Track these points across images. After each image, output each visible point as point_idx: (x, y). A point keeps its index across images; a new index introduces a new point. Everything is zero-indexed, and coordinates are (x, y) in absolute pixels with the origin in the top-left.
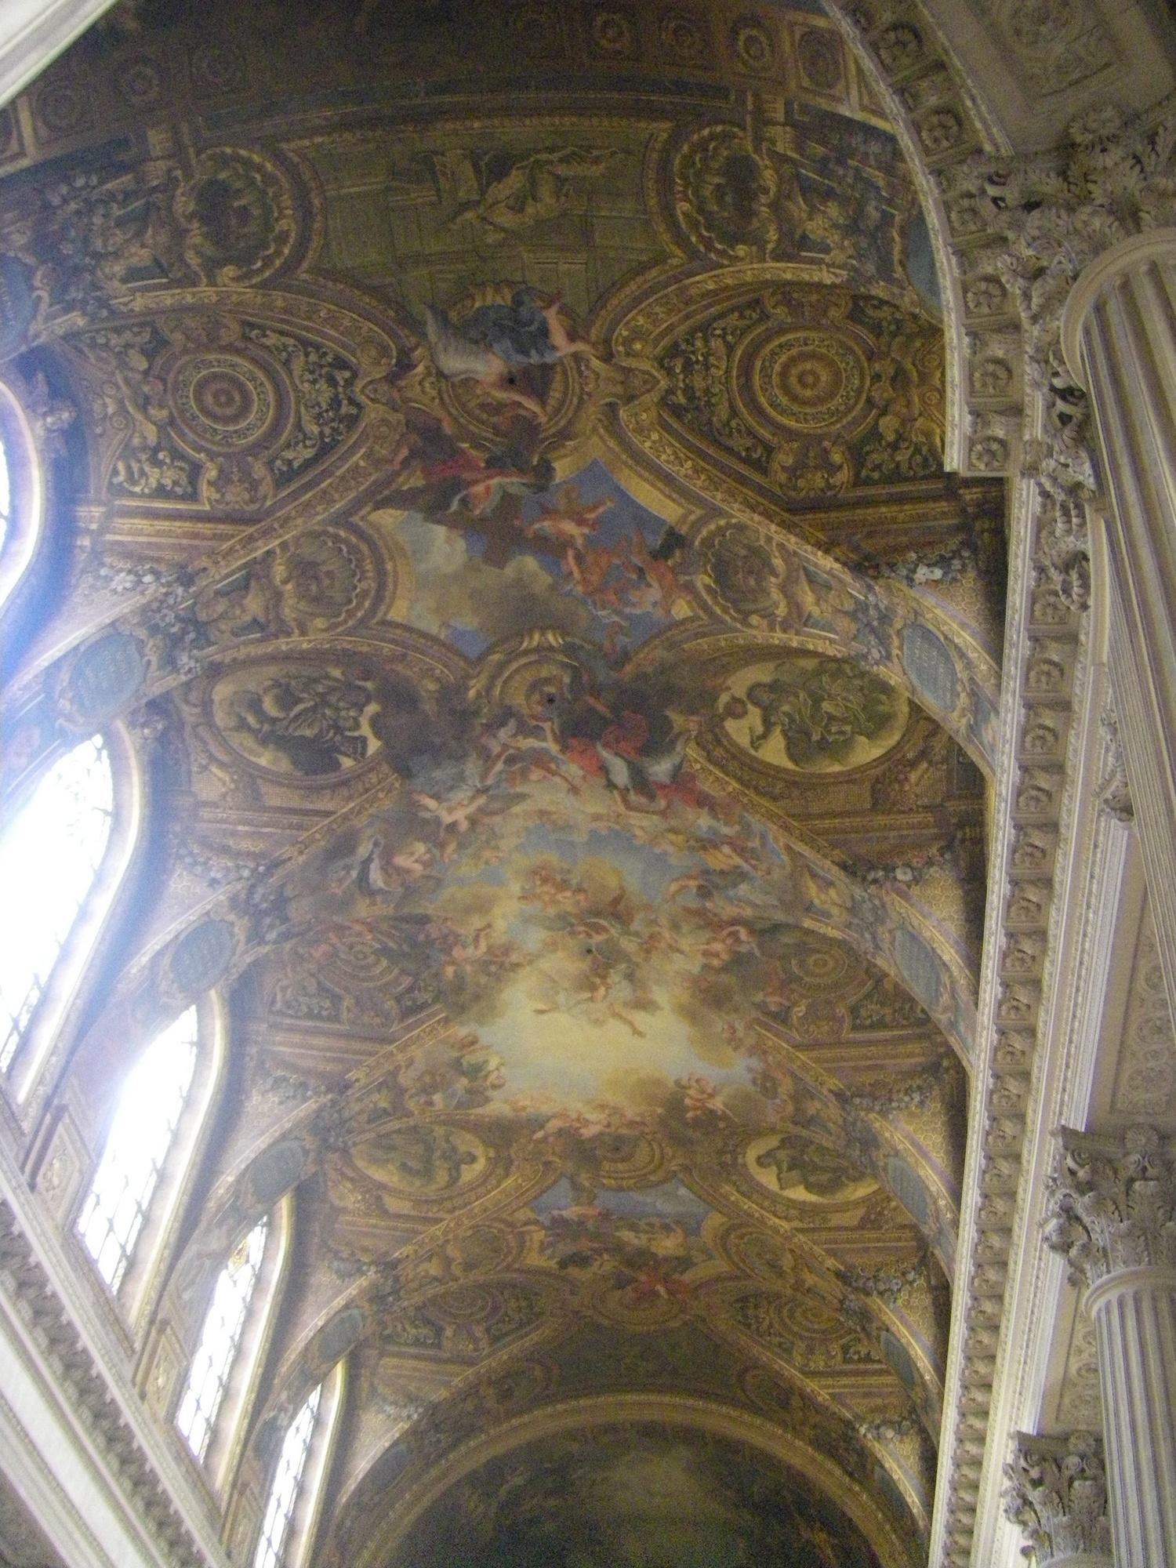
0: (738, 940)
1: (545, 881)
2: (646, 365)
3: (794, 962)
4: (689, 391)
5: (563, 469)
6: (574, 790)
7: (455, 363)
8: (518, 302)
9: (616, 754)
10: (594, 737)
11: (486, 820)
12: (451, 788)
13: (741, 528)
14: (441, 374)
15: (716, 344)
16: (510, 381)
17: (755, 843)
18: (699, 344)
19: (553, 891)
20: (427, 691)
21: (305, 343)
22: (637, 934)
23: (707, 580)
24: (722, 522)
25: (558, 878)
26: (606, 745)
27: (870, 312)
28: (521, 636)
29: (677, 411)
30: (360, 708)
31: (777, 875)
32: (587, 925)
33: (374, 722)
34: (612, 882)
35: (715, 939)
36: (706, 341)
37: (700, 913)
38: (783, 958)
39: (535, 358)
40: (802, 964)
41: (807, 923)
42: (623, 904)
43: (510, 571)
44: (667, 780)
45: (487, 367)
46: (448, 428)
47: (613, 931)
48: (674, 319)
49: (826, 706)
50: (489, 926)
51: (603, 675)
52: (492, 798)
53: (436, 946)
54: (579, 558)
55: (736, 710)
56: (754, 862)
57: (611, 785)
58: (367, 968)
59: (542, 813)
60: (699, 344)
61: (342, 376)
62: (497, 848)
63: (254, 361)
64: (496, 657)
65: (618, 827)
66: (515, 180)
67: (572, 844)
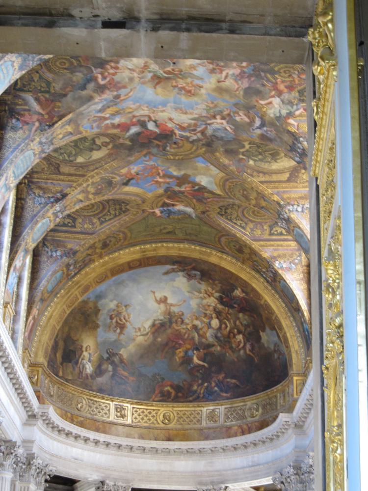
0: (102, 74)
1: (190, 92)
3: (76, 64)
4: (120, 205)
5: (161, 191)
6: (171, 119)
7: (189, 210)
9: (151, 131)
10: (160, 134)
11: (209, 116)
12: (219, 129)
13: (104, 195)
14: (194, 209)
16: (173, 205)
17: (95, 125)
18: (117, 213)
19: (187, 87)
20: (220, 153)
21: (231, 220)
22: (150, 72)
23: (115, 180)
24: (110, 194)
25: (183, 92)
26: (156, 132)
27: (71, 221)
28: (182, 159)
29: (123, 202)
30: (247, 151)
31: (86, 120)
32: (173, 74)
33: (244, 147)
34: (159, 89)
35: (114, 74)
36: (115, 213)
37: (120, 88)
38: (81, 66)
39: (165, 209)
40: (72, 63)
41: (70, 116)
42: (155, 83)
43: (182, 173)
44: (132, 127)
45: (180, 207)
46: (194, 200)
47: (162, 72)
48: (124, 218)
49: (72, 144)
50: (219, 82)
51: (154, 150)
52: (204, 121)
53: (247, 75)
54: (159, 174)
55: (106, 144)
56: (95, 118)
57: (155, 122)
58: (286, 67)
59: (186, 113)
60: (117, 213)
62: (207, 106)
63: (247, 218)
64: (192, 156)
65: (154, 109)
66: (165, 231)
67: (175, 103)
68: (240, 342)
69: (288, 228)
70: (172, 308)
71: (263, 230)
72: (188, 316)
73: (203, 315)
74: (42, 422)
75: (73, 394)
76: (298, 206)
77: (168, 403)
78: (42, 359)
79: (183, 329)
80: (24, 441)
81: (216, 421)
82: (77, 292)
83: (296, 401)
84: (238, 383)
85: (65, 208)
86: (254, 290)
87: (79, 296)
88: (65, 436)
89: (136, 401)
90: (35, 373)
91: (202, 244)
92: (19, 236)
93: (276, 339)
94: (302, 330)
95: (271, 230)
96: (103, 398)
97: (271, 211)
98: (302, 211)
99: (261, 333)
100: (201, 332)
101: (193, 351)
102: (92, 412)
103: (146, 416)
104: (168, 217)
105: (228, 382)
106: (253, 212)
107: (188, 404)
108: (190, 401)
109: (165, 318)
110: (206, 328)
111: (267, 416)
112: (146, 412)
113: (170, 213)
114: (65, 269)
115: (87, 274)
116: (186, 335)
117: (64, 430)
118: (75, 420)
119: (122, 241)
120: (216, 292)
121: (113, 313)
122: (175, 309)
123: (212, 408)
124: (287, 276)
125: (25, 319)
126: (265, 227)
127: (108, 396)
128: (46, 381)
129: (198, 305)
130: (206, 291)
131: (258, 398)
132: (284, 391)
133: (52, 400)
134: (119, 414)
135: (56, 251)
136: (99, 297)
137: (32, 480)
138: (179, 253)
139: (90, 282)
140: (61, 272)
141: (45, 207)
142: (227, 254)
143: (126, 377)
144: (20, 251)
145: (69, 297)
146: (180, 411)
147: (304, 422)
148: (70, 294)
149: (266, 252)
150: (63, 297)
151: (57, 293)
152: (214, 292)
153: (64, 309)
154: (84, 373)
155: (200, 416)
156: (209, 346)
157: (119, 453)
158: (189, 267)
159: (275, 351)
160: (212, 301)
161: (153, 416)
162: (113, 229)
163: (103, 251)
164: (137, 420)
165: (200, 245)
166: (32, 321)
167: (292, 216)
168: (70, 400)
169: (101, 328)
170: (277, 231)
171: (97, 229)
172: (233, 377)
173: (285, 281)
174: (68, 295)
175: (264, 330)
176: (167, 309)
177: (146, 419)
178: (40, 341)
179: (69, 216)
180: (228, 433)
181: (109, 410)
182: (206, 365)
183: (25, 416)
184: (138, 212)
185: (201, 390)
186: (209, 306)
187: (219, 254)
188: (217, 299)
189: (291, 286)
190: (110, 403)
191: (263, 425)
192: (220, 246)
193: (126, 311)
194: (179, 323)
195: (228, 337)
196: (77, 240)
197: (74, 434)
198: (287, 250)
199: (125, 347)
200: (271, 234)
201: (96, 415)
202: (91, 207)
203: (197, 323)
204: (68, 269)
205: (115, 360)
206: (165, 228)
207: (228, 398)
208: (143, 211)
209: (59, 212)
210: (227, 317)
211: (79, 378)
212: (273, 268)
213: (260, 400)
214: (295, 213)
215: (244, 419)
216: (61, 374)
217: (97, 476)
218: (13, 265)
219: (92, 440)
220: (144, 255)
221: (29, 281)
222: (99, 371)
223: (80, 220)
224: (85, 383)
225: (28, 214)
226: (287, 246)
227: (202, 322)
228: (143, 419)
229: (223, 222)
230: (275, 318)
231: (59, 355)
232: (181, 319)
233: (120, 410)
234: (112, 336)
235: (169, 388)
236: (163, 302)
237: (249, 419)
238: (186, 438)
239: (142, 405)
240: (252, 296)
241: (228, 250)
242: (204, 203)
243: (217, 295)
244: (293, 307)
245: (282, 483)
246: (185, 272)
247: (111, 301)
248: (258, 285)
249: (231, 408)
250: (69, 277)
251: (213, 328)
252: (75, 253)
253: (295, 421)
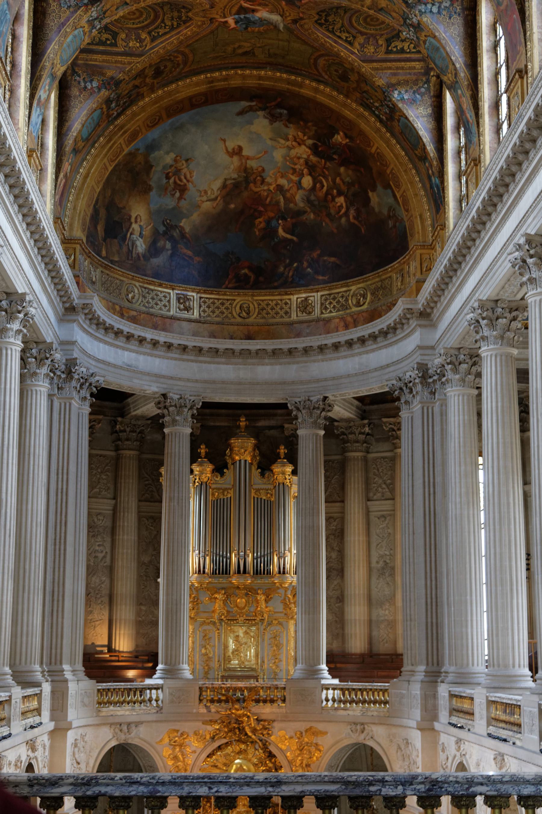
2: (197, 18)
4: (179, 11)
7: (275, 18)
8: (246, 28)
14: (282, 16)
15: (169, 23)
16: (254, 11)
18: (175, 23)
21: (333, 32)
27: (110, 37)
29: (184, 7)
36: (172, 25)
39: (242, 16)
45: (263, 14)
48: (185, 31)
60: (175, 23)
61: (323, 21)
63: (356, 29)
66: (240, 51)
68: (341, 206)
69: (417, 38)
70: (248, 162)
71: (378, 46)
72: (272, 172)
73: (291, 171)
74: (83, 317)
75: (121, 280)
76: (433, 5)
77: (246, 291)
78: (78, 233)
79: (264, 190)
80: (62, 343)
81: (310, 313)
82: (121, 140)
83: (420, 283)
84: (338, 262)
85: (104, 13)
86: (362, 133)
87: (124, 146)
88: (113, 335)
89: (204, 288)
90: (71, 251)
91: (291, 70)
92: (43, 54)
93: (391, 200)
94: (428, 186)
95: (388, 46)
96: (160, 285)
97: (394, 14)
98: (439, 12)
99: (370, 194)
100: (288, 195)
101: (278, 221)
102: (147, 304)
103: (218, 308)
104: (246, 28)
105: (325, 261)
106: (365, 20)
107: (272, 291)
108: (276, 288)
109: (239, 176)
110: (295, 189)
111: (379, 304)
112: (218, 303)
113: (248, 23)
114: (104, 106)
115: (134, 115)
116: (268, 199)
117: (112, 327)
118: (125, 314)
119: (181, 66)
120: (309, 138)
121: (170, 170)
122: (252, 164)
123: (304, 295)
124: (410, 112)
125: (54, 177)
126: (380, 42)
127: (167, 283)
128: (86, 263)
129: (284, 158)
130: (294, 137)
131: (367, 281)
132: (402, 270)
133: (94, 289)
134: (182, 306)
135: (91, 81)
136: (152, 147)
137: (75, 393)
138: (259, 84)
139: (139, 126)
140: (99, 111)
141: (76, 11)
142: (326, 84)
143: (190, 257)
144: (44, 77)
145: (111, 148)
146: (263, 301)
147: (432, 308)
148: (112, 142)
149: (381, 78)
150: (103, 147)
151: (95, 142)
152: (305, 138)
153: (104, 164)
154: (134, 252)
155: (288, 306)
156: (300, 213)
157: (185, 357)
158: (273, 103)
159: (389, 217)
160: (303, 151)
161: (227, 308)
162: (169, 48)
163: (155, 81)
164: (206, 314)
165: (286, 72)
166: (64, 181)
167: (425, 19)
168: (117, 288)
169: (154, 191)
170: (396, 47)
171: (147, 48)
172: (330, 255)
173: (406, 118)
174: (110, 145)
175: (374, 189)
176: (242, 163)
177: (217, 312)
178: (75, 208)
179: (106, 28)
180: (325, 325)
181: (169, 301)
182: (295, 238)
183: (60, 308)
184: (204, 23)
185: (289, 273)
186: (299, 158)
187: (314, 84)
188: (309, 148)
189: (415, 125)
190: (171, 291)
191: (373, 315)
192: (316, 73)
193: (187, 167)
194: (259, 183)
195: (325, 199)
196: (119, 65)
197: (125, 333)
198: (410, 74)
199: (187, 217)
200: (388, 52)
201: (152, 307)
202: (137, 14)
203: (283, 182)
204: (109, 108)
205: (175, 234)
206: (240, 47)
207: (325, 282)
208: (212, 20)
209: (95, 19)
210: (324, 172)
211: (128, 259)
212: (390, 101)
213: (369, 283)
214: (428, 15)
215: (347, 308)
216: (104, 253)
217: (157, 387)
218: (37, 97)
219: (148, 340)
220: (211, 87)
221: (56, 124)
222: (153, 250)
223: (123, 36)
224: (136, 266)
225: (52, 22)
226: (410, 68)
227: (290, 181)
228: (213, 312)
229: (322, 36)
230: (391, 172)
231: (100, 228)
232: (261, 176)
233: (182, 300)
234: (169, 202)
235: (246, 271)
236: (236, 154)
237: (354, 309)
238: (271, 335)
239: (212, 294)
240: (358, 142)
241: (326, 77)
242: (296, 6)
243: (310, 142)
244: (416, 155)
245: (401, 389)
246: (268, 111)
247: (168, 153)
248: (369, 124)
249: (330, 295)
250: (110, 119)
251: (304, 189)
252: (118, 83)
253: (420, 306)
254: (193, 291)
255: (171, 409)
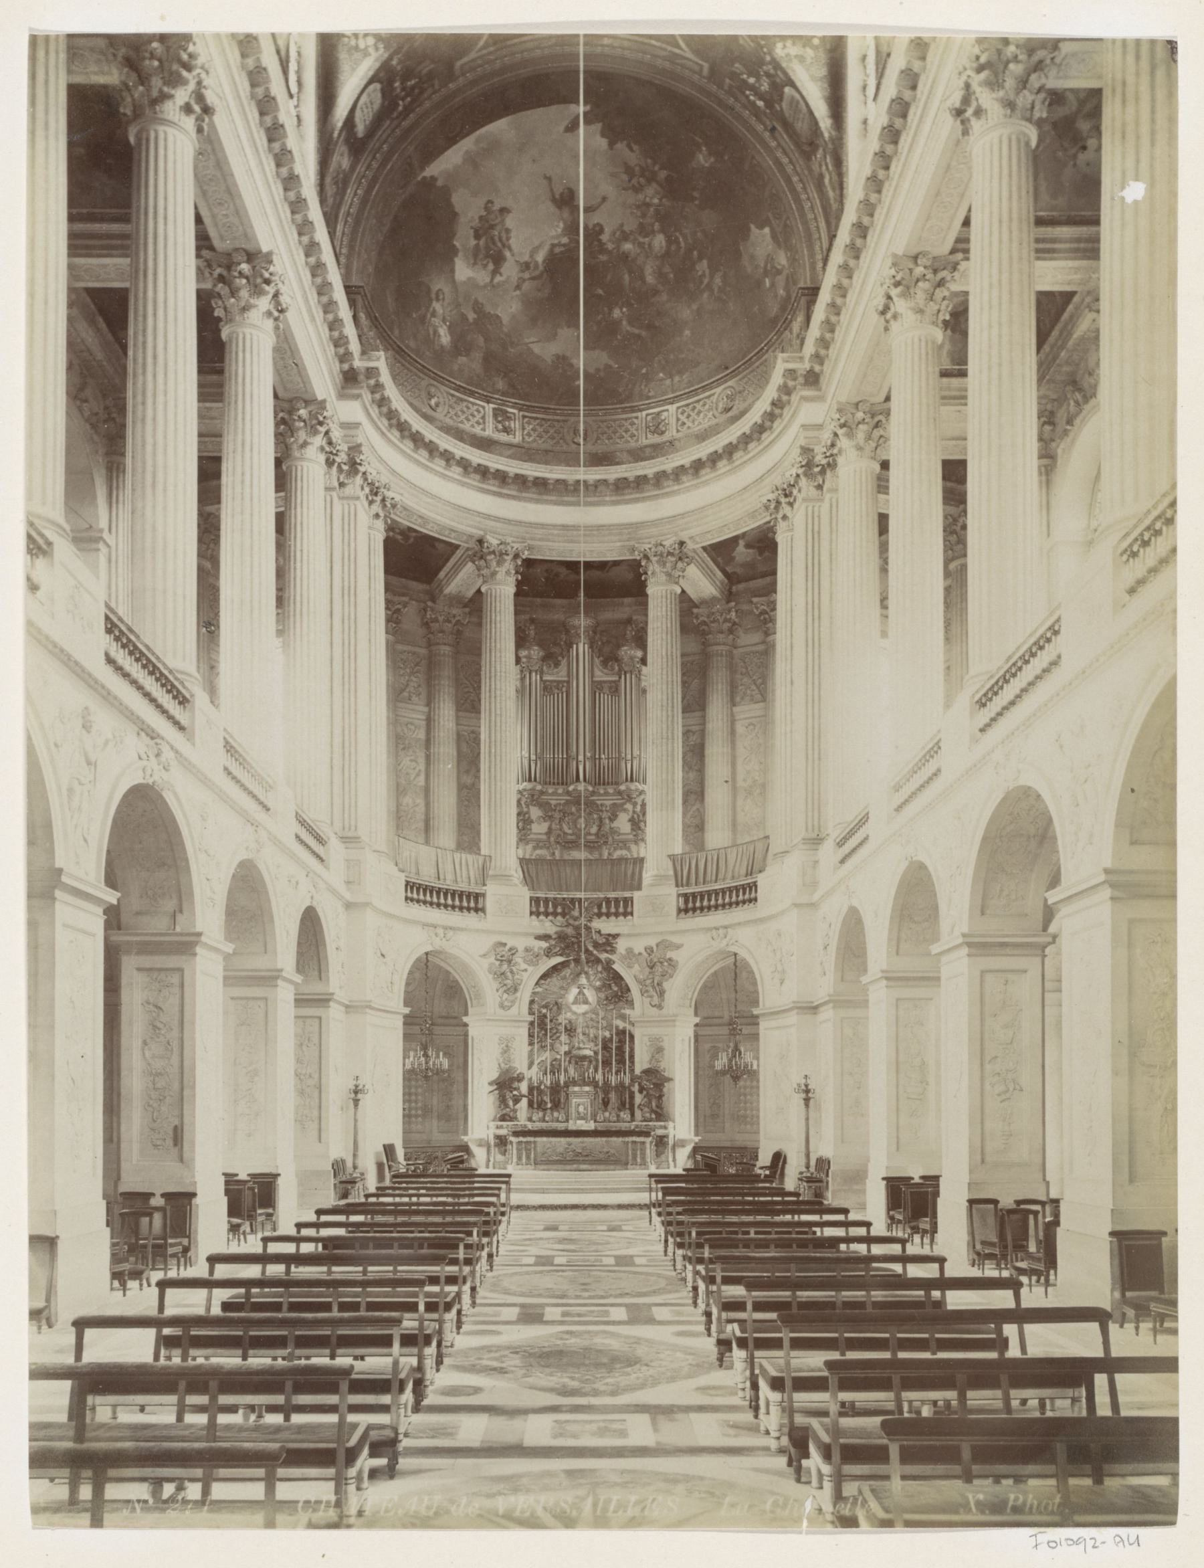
81: (663, 433)
134: (500, 427)
169: (460, 254)
222: (461, 345)
254: (515, 406)
255: (489, 558)
